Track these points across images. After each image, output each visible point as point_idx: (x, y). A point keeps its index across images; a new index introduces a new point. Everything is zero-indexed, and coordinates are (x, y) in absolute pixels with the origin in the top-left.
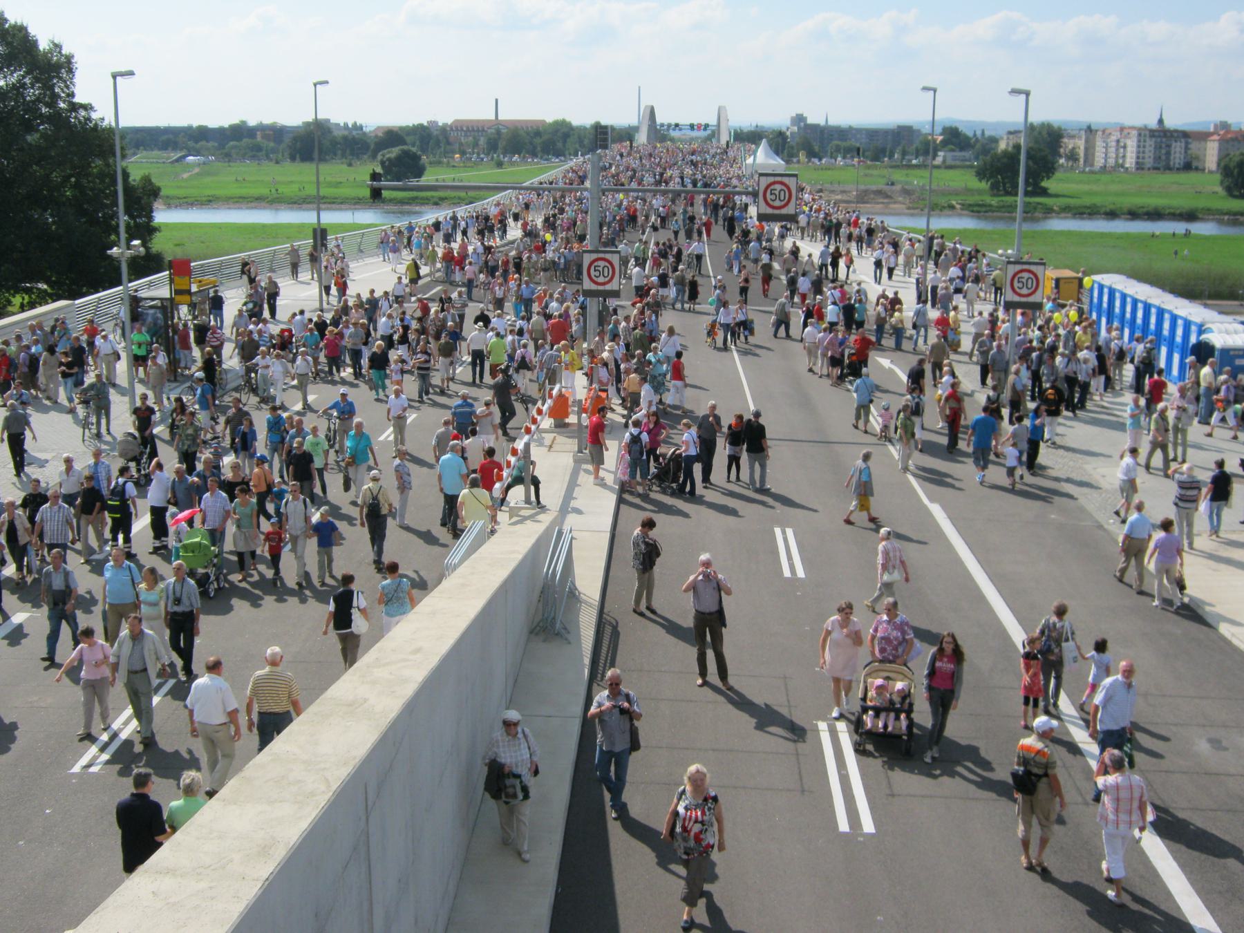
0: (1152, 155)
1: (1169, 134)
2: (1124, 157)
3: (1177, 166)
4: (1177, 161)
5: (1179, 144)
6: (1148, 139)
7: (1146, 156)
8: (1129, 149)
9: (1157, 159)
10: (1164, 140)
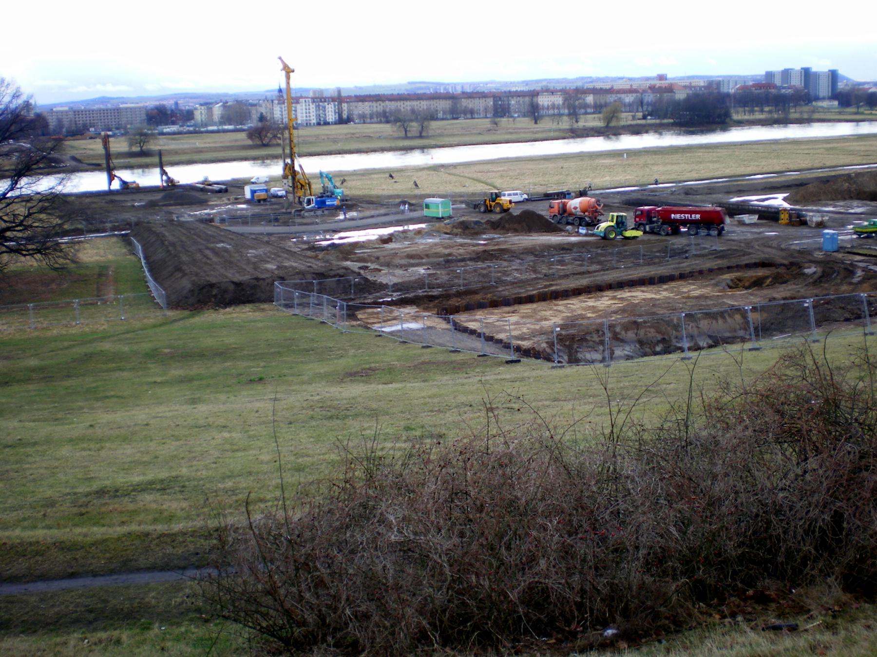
0: (314, 114)
1: (323, 100)
3: (331, 120)
4: (330, 117)
5: (330, 106)
6: (311, 104)
7: (311, 115)
8: (299, 111)
9: (318, 116)
10: (321, 104)
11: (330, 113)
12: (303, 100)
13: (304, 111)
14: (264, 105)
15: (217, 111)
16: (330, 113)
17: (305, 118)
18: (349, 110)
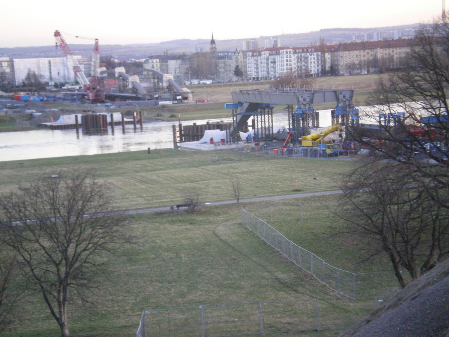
1: (305, 50)
5: (312, 57)
6: (292, 55)
8: (278, 63)
10: (303, 55)
11: (313, 65)
12: (285, 51)
13: (285, 63)
14: (234, 58)
16: (313, 65)
17: (285, 71)
18: (332, 61)
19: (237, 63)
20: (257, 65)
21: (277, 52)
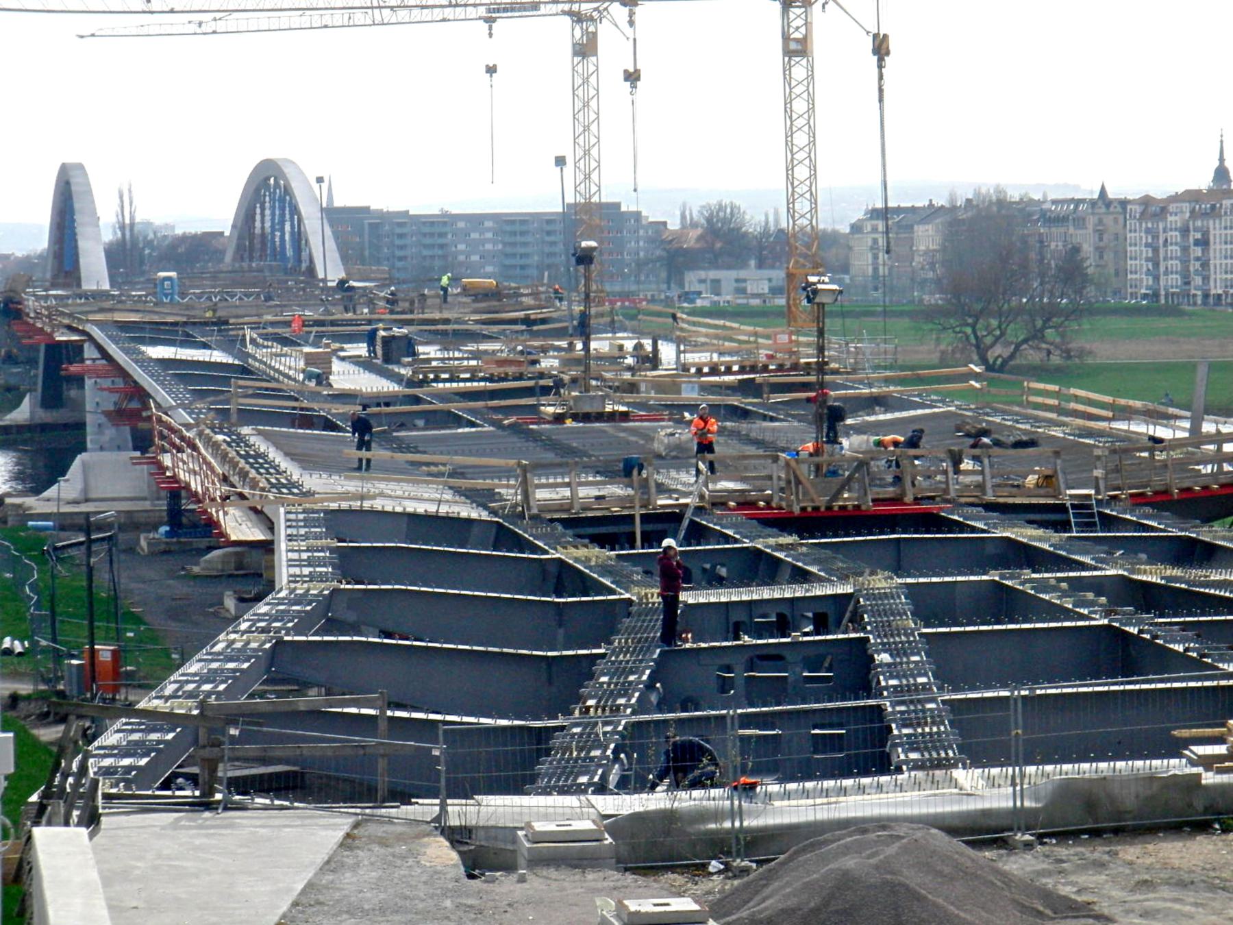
2: (1205, 265)
14: (1091, 221)
15: (927, 238)
19: (1101, 239)
20: (1156, 251)
21: (1213, 207)
